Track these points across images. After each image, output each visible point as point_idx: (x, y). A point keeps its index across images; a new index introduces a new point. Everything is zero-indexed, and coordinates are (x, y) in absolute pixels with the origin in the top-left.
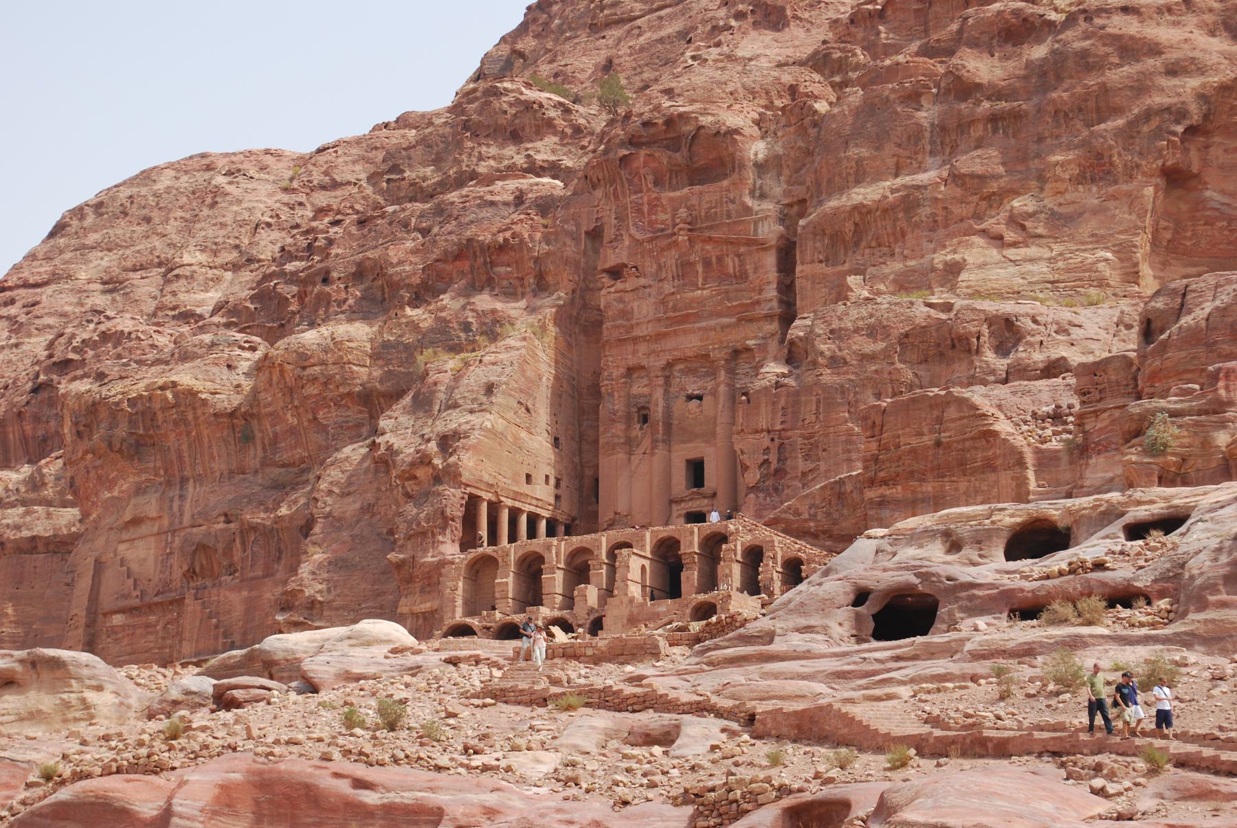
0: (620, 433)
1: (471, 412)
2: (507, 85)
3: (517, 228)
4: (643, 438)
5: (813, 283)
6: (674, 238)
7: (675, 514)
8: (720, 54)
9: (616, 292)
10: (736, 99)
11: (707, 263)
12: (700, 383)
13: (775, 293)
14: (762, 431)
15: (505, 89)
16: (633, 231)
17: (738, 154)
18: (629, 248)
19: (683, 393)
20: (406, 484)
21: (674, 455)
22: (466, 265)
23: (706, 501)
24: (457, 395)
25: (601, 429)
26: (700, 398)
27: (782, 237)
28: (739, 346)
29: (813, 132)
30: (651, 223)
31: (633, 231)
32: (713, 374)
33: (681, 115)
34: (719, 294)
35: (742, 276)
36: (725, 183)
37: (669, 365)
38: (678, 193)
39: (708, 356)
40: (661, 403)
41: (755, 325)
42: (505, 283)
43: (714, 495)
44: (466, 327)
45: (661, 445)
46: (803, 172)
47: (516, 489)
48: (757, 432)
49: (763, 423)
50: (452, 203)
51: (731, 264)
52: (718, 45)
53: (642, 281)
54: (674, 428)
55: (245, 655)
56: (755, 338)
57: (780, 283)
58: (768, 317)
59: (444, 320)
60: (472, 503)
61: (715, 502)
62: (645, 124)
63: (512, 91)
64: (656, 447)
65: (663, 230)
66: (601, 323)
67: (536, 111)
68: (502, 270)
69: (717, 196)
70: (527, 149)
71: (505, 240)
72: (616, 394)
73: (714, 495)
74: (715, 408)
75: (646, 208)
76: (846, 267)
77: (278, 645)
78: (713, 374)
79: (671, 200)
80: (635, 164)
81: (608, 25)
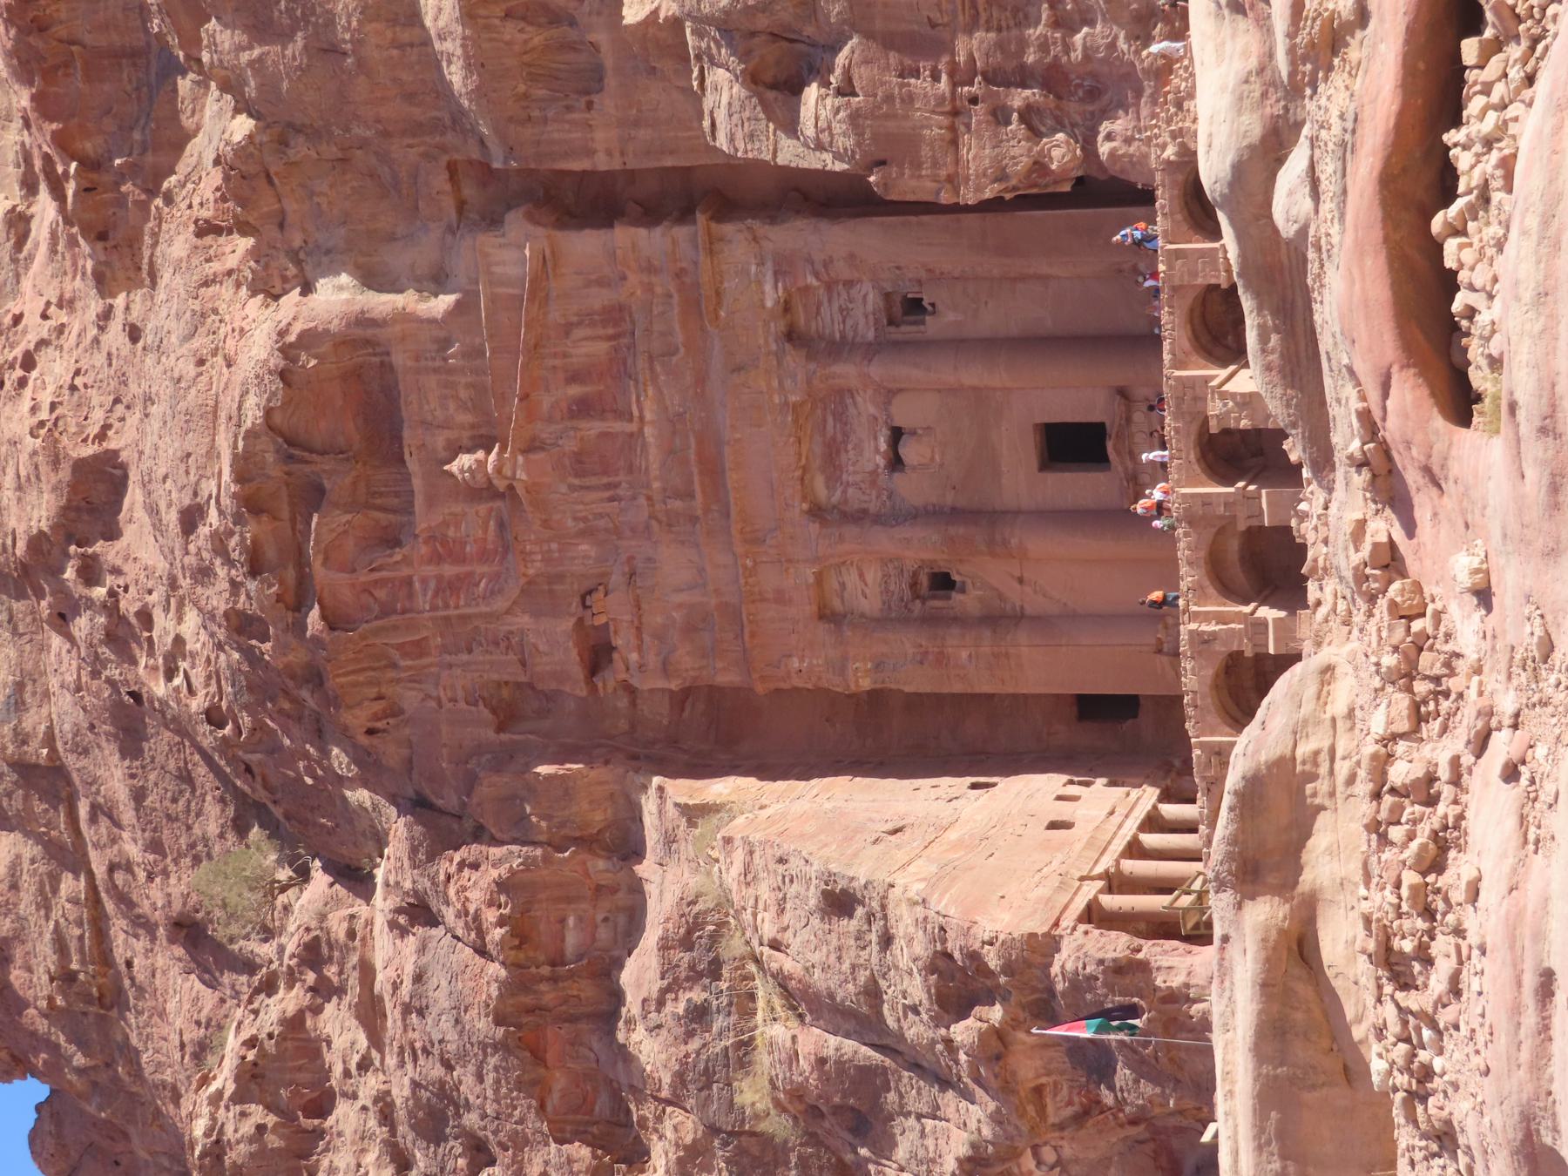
1: (887, 941)
2: (199, 1128)
3: (476, 897)
5: (636, 124)
6: (520, 491)
8: (167, 609)
9: (640, 649)
10: (215, 353)
11: (583, 408)
13: (658, 232)
14: (952, 128)
15: (207, 1135)
16: (500, 604)
17: (334, 326)
18: (537, 614)
19: (883, 477)
20: (1052, 1119)
22: (555, 1037)
24: (847, 993)
25: (958, 688)
26: (897, 434)
27: (530, 217)
28: (778, 327)
29: (300, 149)
30: (484, 556)
31: (500, 604)
33: (240, 477)
34: (654, 378)
35: (615, 315)
36: (399, 359)
37: (817, 512)
38: (417, 483)
41: (730, 285)
42: (604, 934)
43: (1123, 393)
44: (699, 1015)
46: (385, 171)
47: (1078, 846)
48: (954, 143)
49: (935, 129)
50: (416, 1085)
51: (590, 348)
52: (146, 617)
53: (616, 579)
55: (1257, 295)
56: (760, 283)
57: (637, 223)
58: (712, 245)
59: (680, 1078)
60: (1093, 915)
62: (254, 571)
63: (213, 1118)
64: (1005, 543)
65: (501, 525)
66: (714, 694)
67: (263, 1053)
68: (572, 940)
69: (431, 382)
70: (347, 1074)
71: (501, 922)
75: (449, 570)
76: (601, 37)
77: (1220, 140)
79: (431, 502)
80: (347, 595)
81: (104, 956)
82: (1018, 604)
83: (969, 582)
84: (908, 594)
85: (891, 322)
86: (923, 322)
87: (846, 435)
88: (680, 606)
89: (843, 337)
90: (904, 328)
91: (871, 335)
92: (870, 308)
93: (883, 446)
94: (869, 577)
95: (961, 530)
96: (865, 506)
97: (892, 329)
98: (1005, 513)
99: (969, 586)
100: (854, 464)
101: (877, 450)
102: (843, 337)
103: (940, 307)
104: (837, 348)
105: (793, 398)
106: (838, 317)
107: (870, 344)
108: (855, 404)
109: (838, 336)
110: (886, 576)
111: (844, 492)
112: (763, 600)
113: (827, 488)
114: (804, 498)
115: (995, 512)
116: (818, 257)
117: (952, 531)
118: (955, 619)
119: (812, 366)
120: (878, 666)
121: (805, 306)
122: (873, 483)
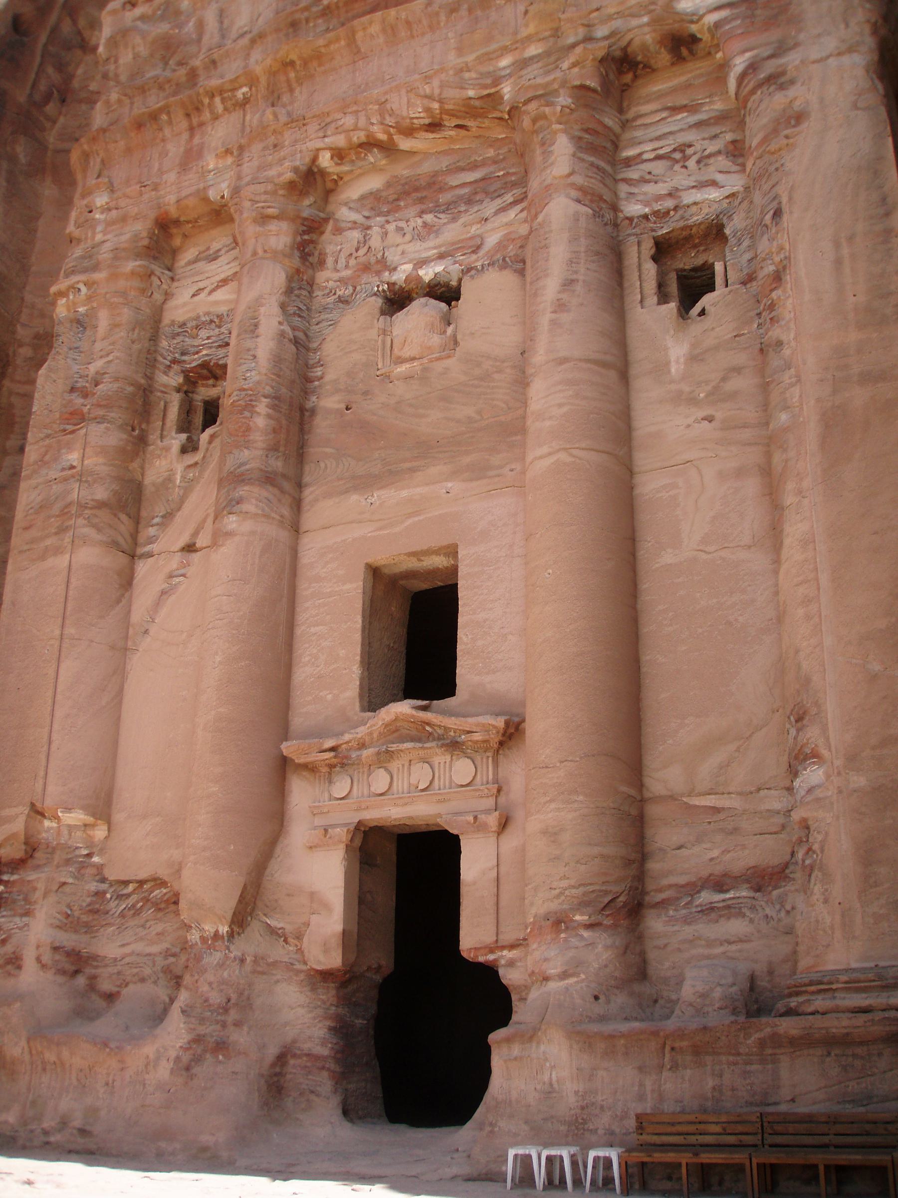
0: (95, 462)
4: (188, 489)
7: (299, 832)
12: (452, 232)
19: (375, 283)
21: (312, 547)
23: (463, 769)
32: (512, 182)
39: (494, 99)
40: (271, 321)
45: (254, 498)
54: (322, 426)
61: (515, 771)
72: (103, 320)
73: (512, 733)
74: (528, 317)
78: (512, 182)
82: (154, 547)
83: (197, 457)
84: (192, 361)
85: (663, 250)
86: (663, 298)
87: (448, 208)
88: (200, 26)
89: (628, 162)
90: (650, 268)
91: (634, 209)
92: (689, 198)
93: (427, 274)
94: (220, 295)
95: (260, 422)
96: (330, 261)
97: (648, 247)
98: (297, 505)
99: (190, 459)
100: (399, 229)
101: (421, 263)
102: (628, 162)
103: (697, 327)
104: (604, 150)
105: (507, 90)
106: (667, 146)
107: (615, 208)
108: (503, 210)
109: (630, 153)
110: (219, 321)
111: (355, 225)
112: (191, 129)
113: (363, 198)
114: (339, 155)
115: (300, 486)
116: (792, 59)
117: (262, 407)
118: (142, 441)
119: (564, 100)
120: (80, 323)
121: (687, 86)
122: (366, 268)
